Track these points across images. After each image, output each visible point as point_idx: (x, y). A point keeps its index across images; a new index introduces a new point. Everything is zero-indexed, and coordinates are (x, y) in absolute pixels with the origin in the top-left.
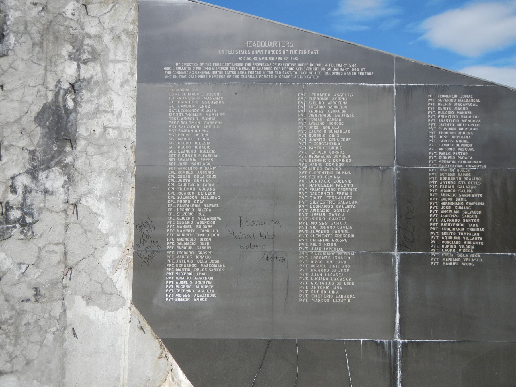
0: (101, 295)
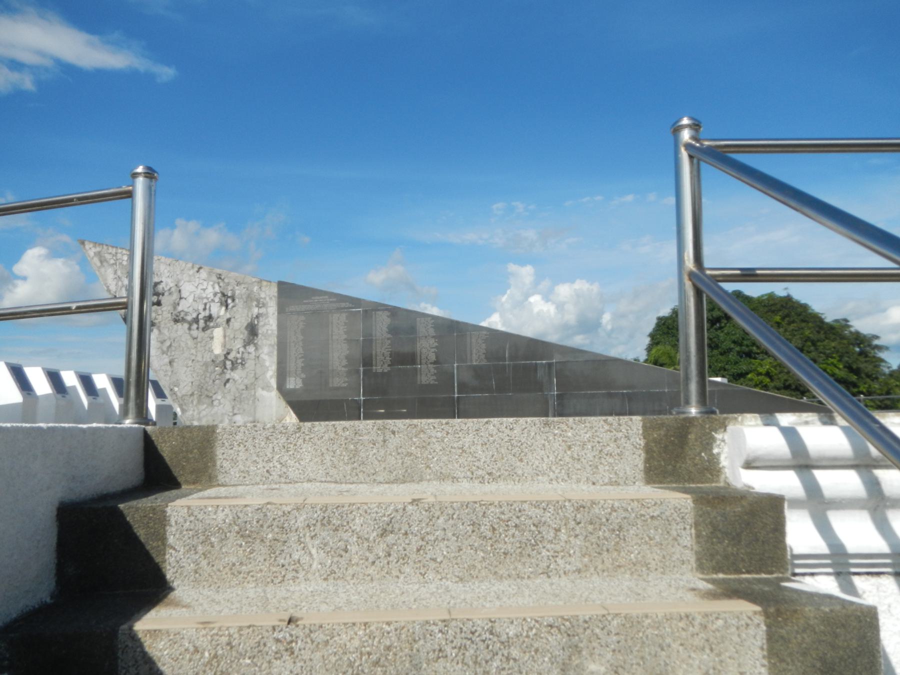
0: (267, 387)
